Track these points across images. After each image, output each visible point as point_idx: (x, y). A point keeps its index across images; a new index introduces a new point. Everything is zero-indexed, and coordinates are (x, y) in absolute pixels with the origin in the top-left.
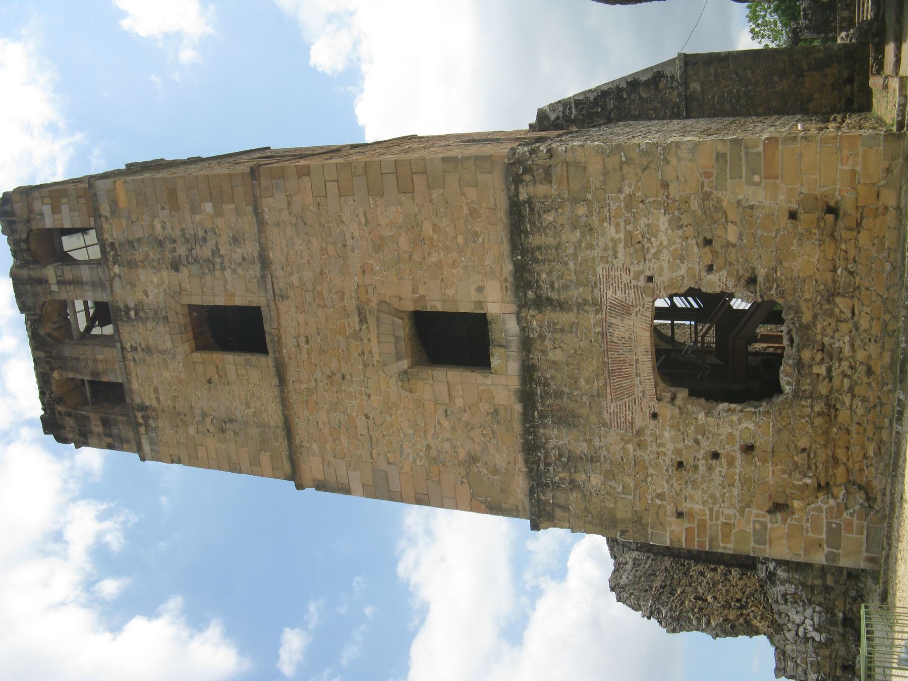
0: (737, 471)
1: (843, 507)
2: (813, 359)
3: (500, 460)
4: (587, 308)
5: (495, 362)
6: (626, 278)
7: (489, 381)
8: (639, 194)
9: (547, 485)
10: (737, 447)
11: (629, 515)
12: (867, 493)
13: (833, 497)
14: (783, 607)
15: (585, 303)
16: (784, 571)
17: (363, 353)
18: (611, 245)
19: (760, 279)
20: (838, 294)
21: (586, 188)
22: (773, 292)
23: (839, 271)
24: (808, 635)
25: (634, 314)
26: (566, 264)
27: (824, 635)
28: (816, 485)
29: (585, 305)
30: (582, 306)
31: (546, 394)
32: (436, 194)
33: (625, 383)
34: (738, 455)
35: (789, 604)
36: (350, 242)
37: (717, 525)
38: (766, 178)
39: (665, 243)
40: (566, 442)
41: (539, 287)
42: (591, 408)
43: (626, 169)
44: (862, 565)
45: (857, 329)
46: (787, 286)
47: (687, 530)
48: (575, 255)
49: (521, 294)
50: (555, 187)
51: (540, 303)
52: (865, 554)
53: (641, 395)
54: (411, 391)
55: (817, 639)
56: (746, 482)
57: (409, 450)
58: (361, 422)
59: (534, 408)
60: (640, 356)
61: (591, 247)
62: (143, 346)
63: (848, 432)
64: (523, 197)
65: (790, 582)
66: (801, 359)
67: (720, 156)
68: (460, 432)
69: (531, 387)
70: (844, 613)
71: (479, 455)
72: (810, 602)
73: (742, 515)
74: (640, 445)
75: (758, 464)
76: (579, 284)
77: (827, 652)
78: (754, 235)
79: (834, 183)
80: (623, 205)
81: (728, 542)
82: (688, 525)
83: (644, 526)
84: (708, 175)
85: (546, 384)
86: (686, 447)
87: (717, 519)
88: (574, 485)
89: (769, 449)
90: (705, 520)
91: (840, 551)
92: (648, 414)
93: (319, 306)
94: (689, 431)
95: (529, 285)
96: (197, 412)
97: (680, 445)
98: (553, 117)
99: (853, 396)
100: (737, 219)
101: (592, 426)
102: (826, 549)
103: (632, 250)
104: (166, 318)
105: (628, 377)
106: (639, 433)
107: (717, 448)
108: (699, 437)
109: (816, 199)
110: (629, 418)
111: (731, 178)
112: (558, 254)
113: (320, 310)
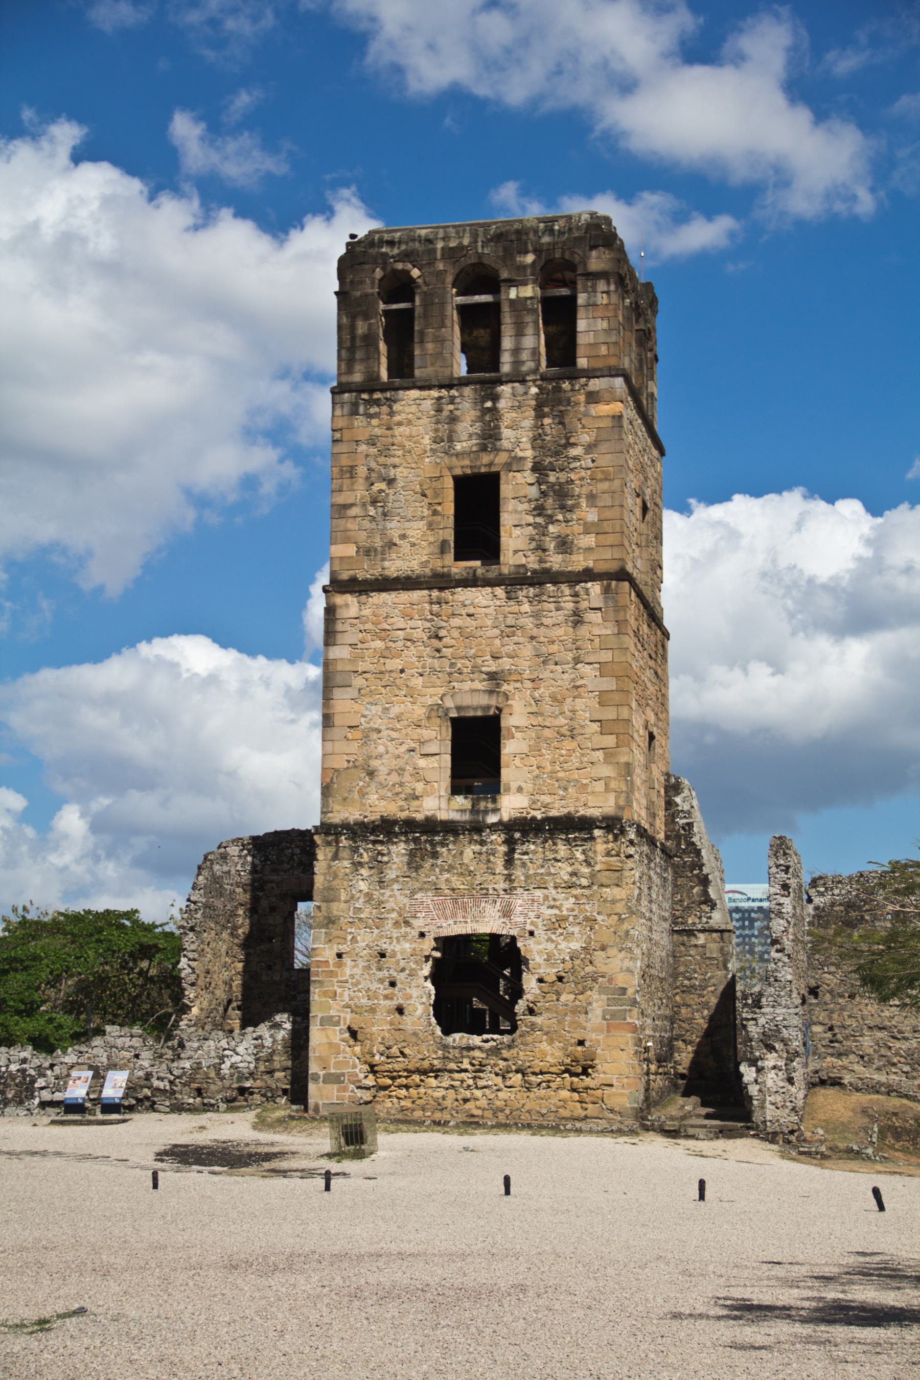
0: (381, 1002)
1: (358, 1084)
2: (474, 1058)
3: (373, 798)
4: (508, 882)
5: (461, 801)
6: (532, 915)
7: (443, 793)
8: (597, 927)
9: (355, 842)
10: (401, 1001)
11: (335, 913)
12: (370, 1102)
13: (366, 1077)
14: (249, 1037)
15: (512, 881)
16: (283, 1037)
17: (460, 674)
18: (558, 903)
19: (533, 1019)
20: (524, 1076)
21: (602, 885)
22: (524, 1028)
23: (540, 1076)
24: (226, 1059)
25: (504, 920)
26: (542, 866)
27: (227, 1072)
28: (374, 1063)
29: (510, 881)
30: (509, 878)
31: (433, 845)
32: (600, 755)
33: (448, 912)
34: (394, 1003)
35: (253, 1042)
36: (558, 667)
37: (333, 986)
38: (608, 1025)
39: (559, 947)
40: (396, 860)
41: (523, 843)
42: (425, 883)
43: (616, 917)
44: (311, 1101)
45: (498, 1090)
46: (529, 1039)
47: (327, 962)
48: (549, 874)
49: (517, 828)
50: (603, 859)
51: (510, 842)
52: (320, 1103)
53: (439, 925)
54: (429, 718)
55: (223, 1066)
56: (372, 1010)
57: (374, 712)
58: (395, 664)
59: (423, 833)
60: (469, 925)
61: (556, 888)
62: (457, 413)
63: (419, 1086)
64: (597, 833)
65: (273, 1042)
66: (473, 1049)
67: (624, 991)
68: (394, 762)
69: (440, 832)
70: (250, 1088)
71: (376, 779)
72: (257, 1060)
73: (344, 1007)
74: (396, 924)
75: (389, 1018)
76: (527, 877)
77: (212, 1074)
78: (566, 1014)
79: (604, 1073)
80: (588, 914)
81: (319, 996)
82: (331, 963)
83: (326, 926)
84: (610, 981)
85: (443, 844)
86: (398, 962)
87: (340, 987)
88: (357, 865)
89: (401, 1027)
90: (337, 976)
91: (321, 1084)
92: (423, 930)
93: (502, 632)
94: (411, 964)
95: (525, 833)
96: (392, 473)
97: (399, 956)
98: (678, 800)
99: (447, 1089)
100: (577, 1003)
101: (410, 883)
102: (321, 1073)
103: (554, 920)
104: (483, 448)
105: (454, 915)
106: (407, 923)
107: (399, 985)
108: (407, 972)
109: (592, 1060)
110: (419, 915)
111: (608, 999)
112: (550, 860)
113: (498, 632)
